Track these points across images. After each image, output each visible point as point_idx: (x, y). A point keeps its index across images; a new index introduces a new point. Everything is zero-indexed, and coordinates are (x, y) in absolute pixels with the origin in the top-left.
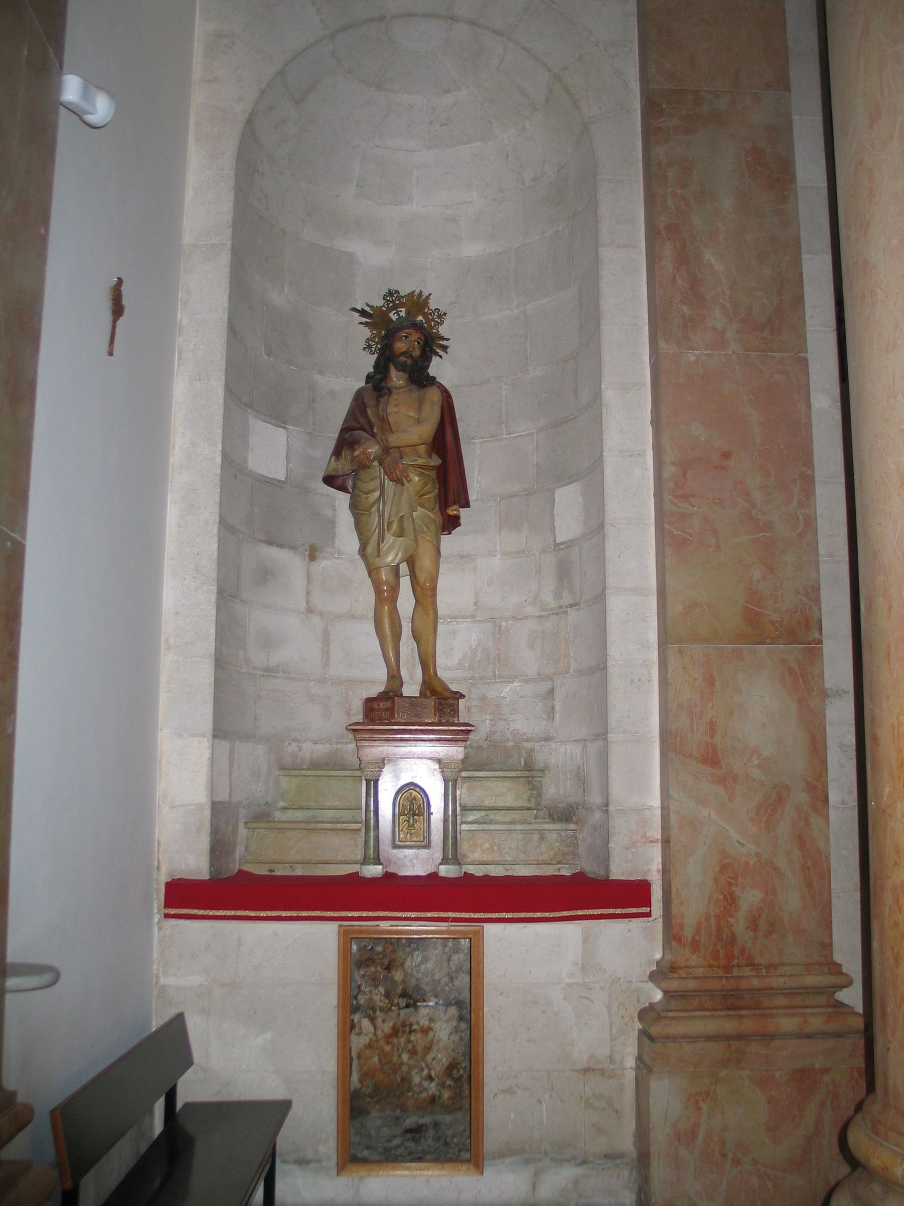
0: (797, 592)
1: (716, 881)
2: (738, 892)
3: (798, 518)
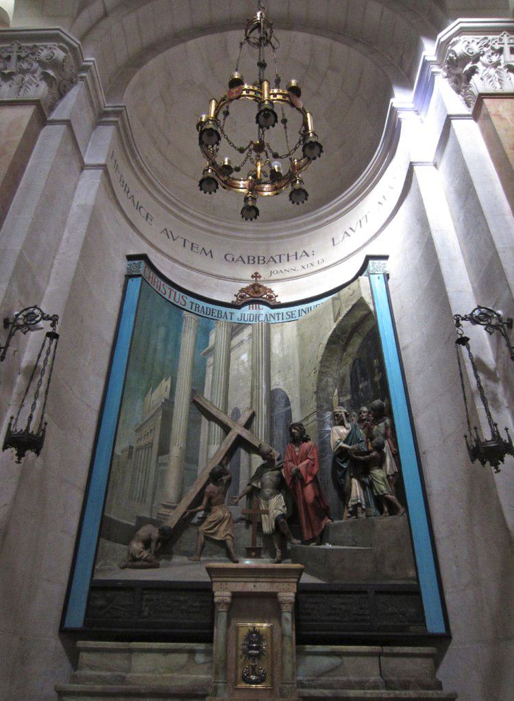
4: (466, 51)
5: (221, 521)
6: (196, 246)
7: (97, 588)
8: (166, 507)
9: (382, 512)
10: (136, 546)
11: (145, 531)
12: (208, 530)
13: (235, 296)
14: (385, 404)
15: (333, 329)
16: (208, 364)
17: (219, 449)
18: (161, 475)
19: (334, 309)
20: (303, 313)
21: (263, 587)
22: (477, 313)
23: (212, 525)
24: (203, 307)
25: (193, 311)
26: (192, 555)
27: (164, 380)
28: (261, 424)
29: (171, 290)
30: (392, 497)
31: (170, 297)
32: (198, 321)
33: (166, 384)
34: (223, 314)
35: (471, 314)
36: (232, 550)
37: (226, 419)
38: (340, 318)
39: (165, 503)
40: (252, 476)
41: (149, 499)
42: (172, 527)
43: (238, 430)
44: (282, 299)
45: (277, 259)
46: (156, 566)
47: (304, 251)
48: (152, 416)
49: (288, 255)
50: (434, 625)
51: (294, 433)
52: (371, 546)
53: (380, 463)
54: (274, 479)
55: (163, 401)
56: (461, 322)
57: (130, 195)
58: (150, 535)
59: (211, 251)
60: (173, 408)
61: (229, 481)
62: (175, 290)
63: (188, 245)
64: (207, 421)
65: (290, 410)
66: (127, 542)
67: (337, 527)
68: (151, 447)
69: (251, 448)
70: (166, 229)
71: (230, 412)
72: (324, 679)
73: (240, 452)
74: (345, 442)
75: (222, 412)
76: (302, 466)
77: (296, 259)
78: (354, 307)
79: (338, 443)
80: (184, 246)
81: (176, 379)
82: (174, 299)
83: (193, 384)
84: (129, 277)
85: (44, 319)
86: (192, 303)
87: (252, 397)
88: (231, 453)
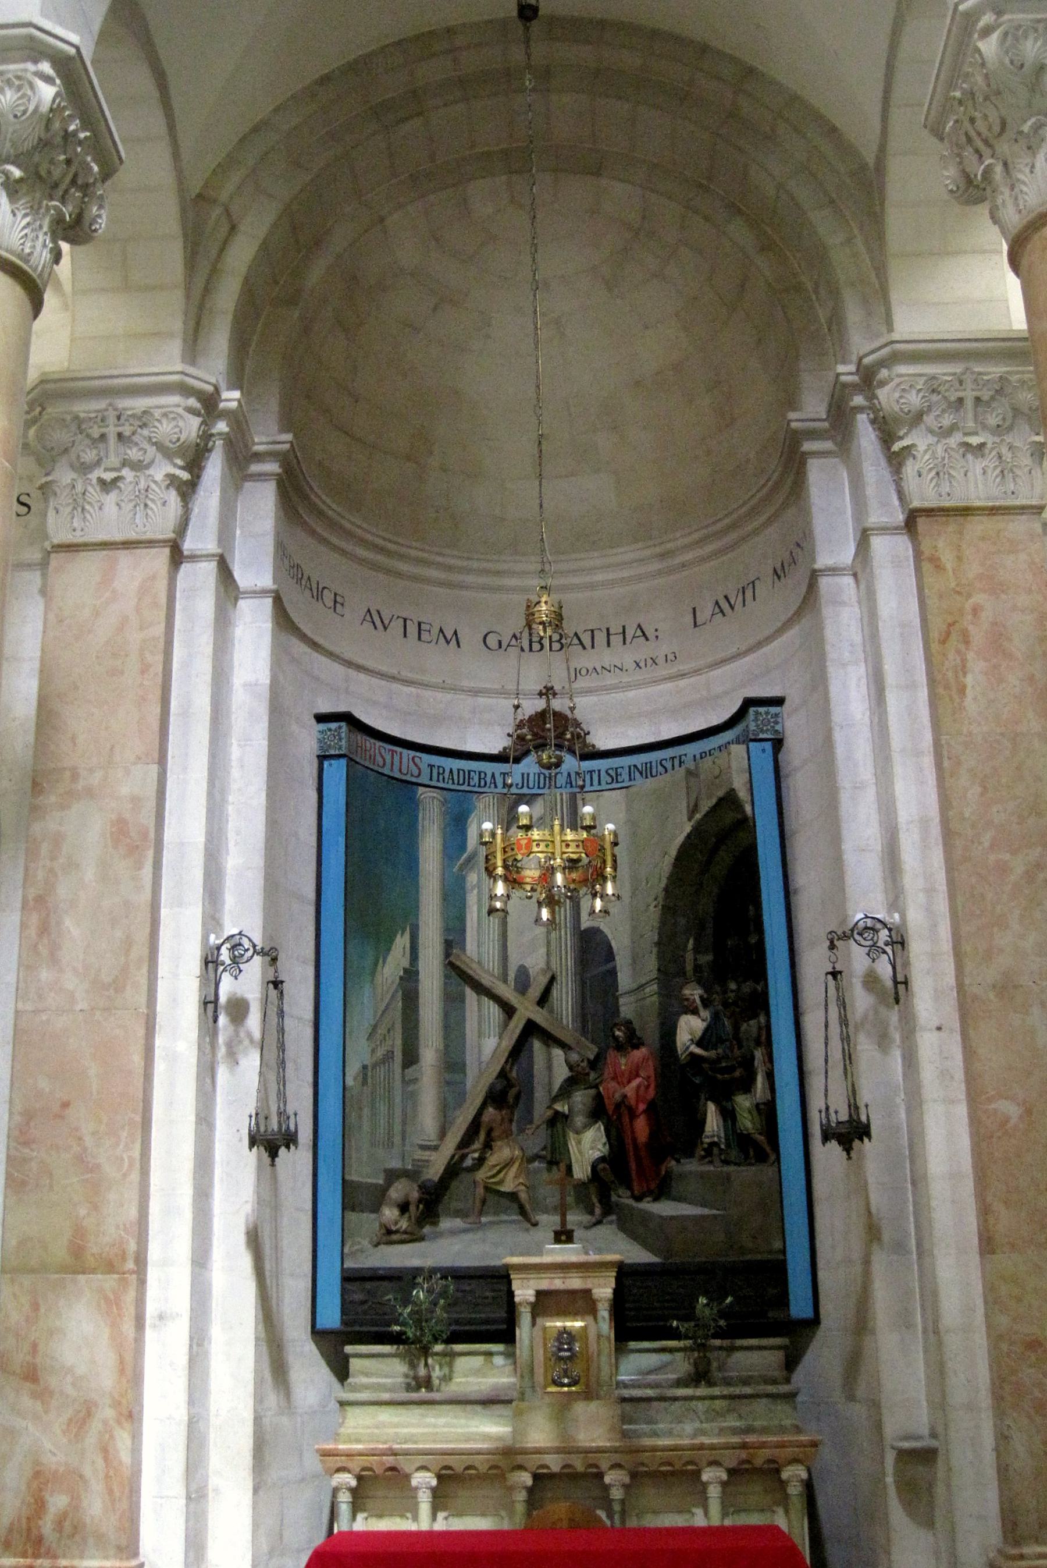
0: (118, 1227)
1: (29, 1487)
2: (47, 1497)
3: (122, 1159)
4: (896, 408)
5: (508, 1165)
6: (428, 627)
7: (350, 1278)
8: (424, 1148)
9: (747, 1157)
10: (390, 1213)
11: (398, 1191)
12: (493, 1176)
13: (509, 735)
14: (759, 988)
15: (685, 834)
16: (468, 885)
17: (499, 1044)
18: (411, 1098)
19: (688, 794)
20: (637, 774)
21: (575, 1282)
22: (861, 924)
23: (498, 1168)
24: (451, 771)
25: (434, 783)
26: (467, 1216)
27: (399, 936)
28: (565, 998)
29: (393, 751)
30: (761, 1138)
31: (392, 770)
32: (443, 803)
33: (402, 942)
34: (488, 779)
35: (852, 930)
36: (528, 1207)
37: (507, 992)
38: (698, 816)
39: (421, 1142)
40: (554, 1093)
41: (397, 1139)
42: (436, 1179)
43: (527, 1010)
44: (603, 739)
45: (586, 639)
46: (422, 1239)
47: (639, 626)
48: (388, 1005)
49: (608, 630)
50: (799, 1307)
51: (618, 1036)
52: (725, 1209)
53: (747, 1085)
54: (588, 1101)
55: (402, 973)
56: (836, 942)
57: (304, 583)
58: (407, 1195)
59: (455, 633)
60: (417, 981)
61: (518, 1097)
62: (399, 749)
63: (412, 629)
64: (474, 995)
65: (615, 968)
66: (376, 1209)
67: (682, 1176)
68: (392, 1058)
69: (550, 1039)
70: (369, 611)
71: (512, 975)
72: (652, 1377)
73: (532, 1043)
74: (700, 1043)
75: (498, 978)
76: (630, 1089)
77: (624, 643)
78: (721, 800)
79: (688, 1048)
80: (405, 636)
81: (417, 926)
82: (400, 771)
83: (447, 930)
84: (322, 758)
85: (258, 954)
86: (431, 766)
87: (549, 943)
88: (518, 1050)
